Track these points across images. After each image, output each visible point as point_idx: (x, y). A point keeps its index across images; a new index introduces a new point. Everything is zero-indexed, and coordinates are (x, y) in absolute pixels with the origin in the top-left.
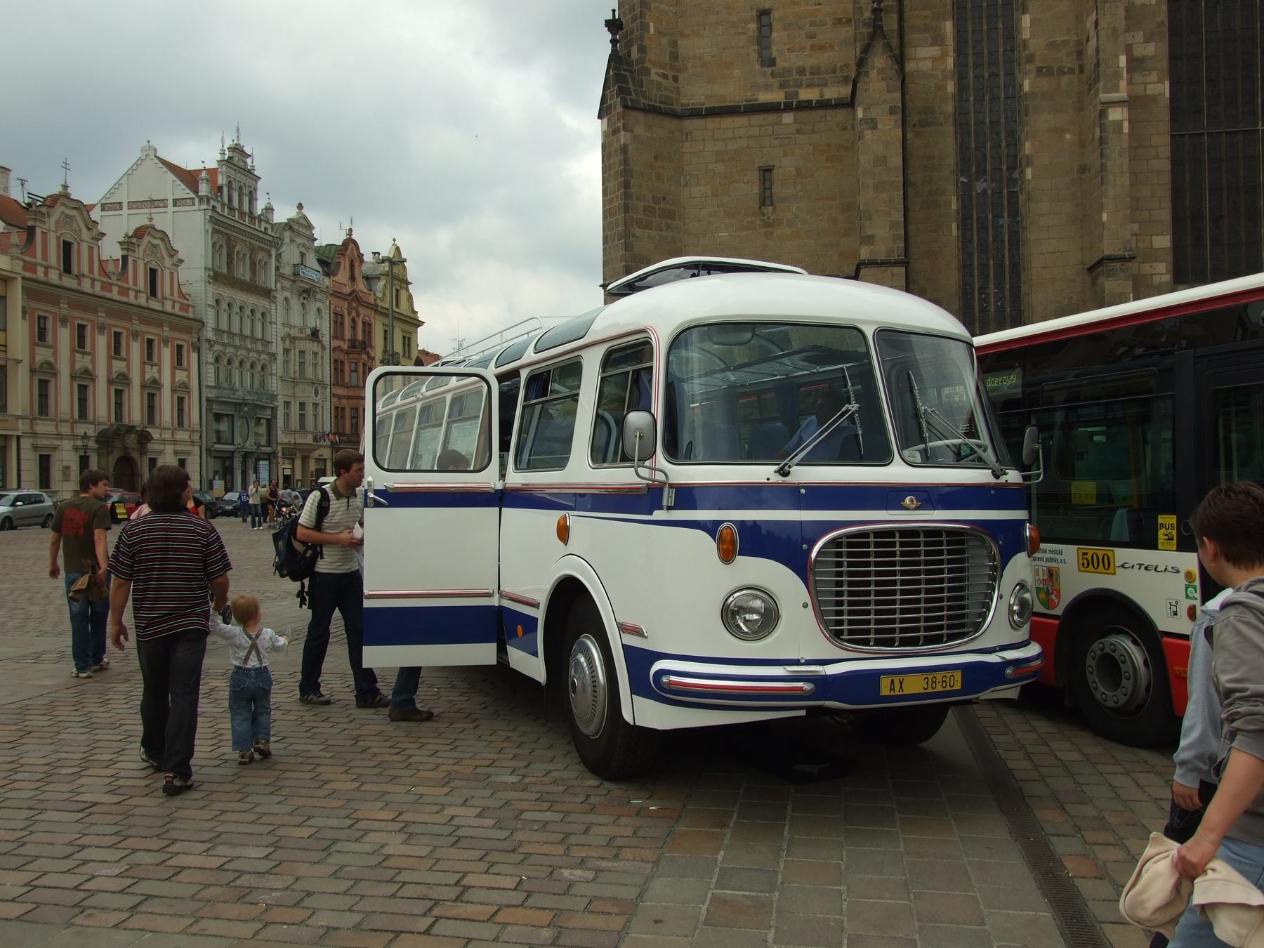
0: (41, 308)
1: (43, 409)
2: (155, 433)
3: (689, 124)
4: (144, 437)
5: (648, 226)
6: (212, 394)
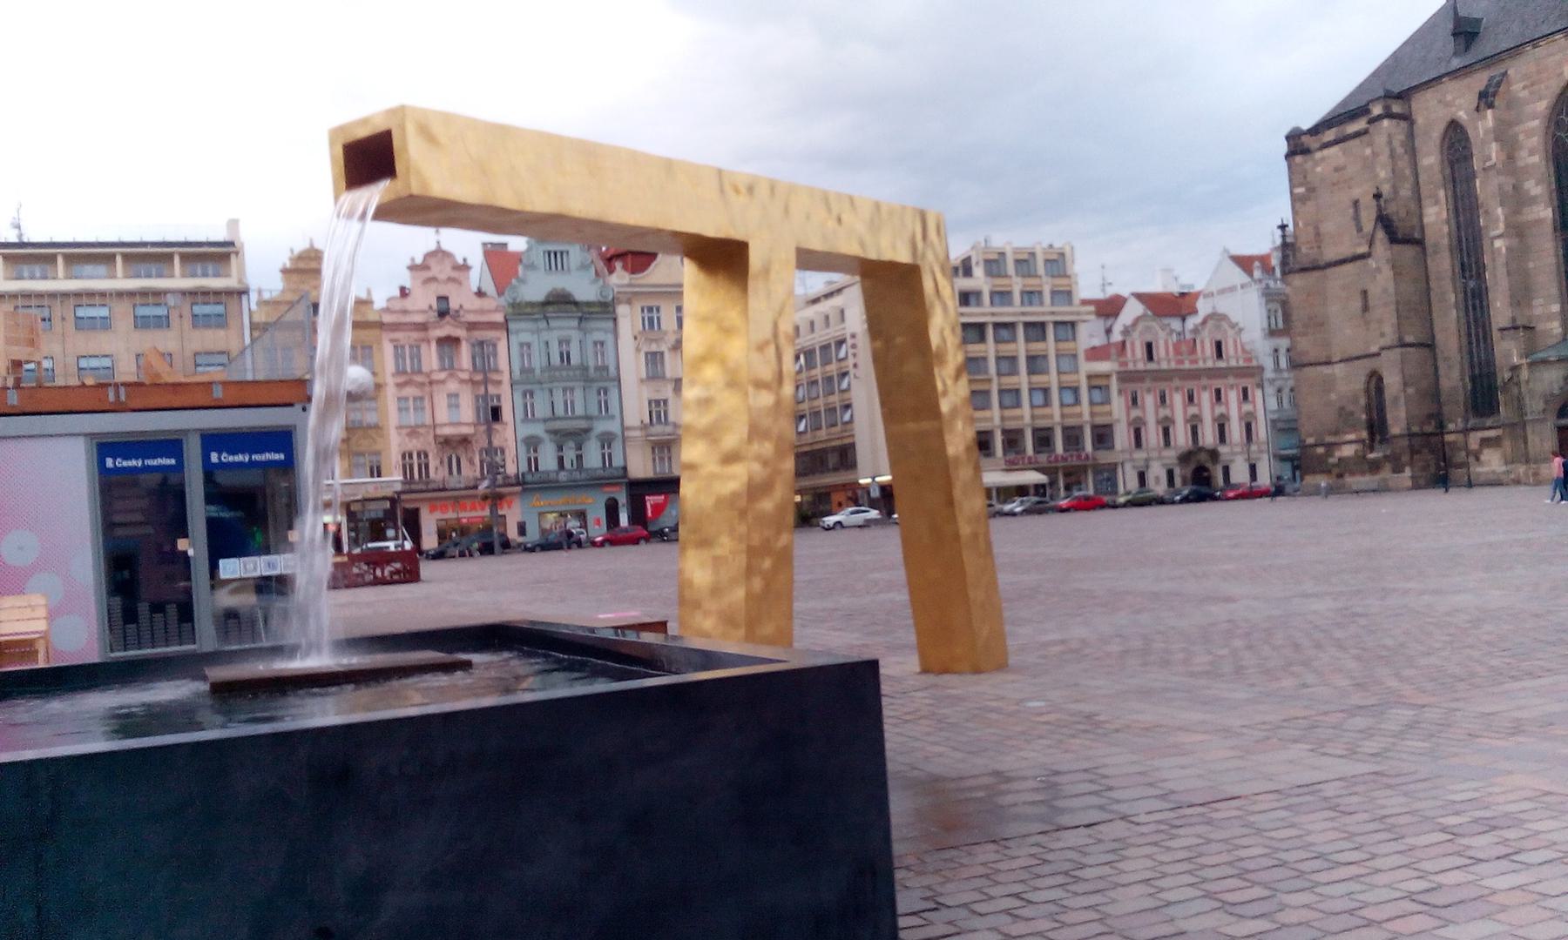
0: (1131, 386)
1: (1138, 444)
2: (1223, 450)
3: (1329, 271)
4: (1214, 455)
5: (1305, 334)
6: (1275, 416)
